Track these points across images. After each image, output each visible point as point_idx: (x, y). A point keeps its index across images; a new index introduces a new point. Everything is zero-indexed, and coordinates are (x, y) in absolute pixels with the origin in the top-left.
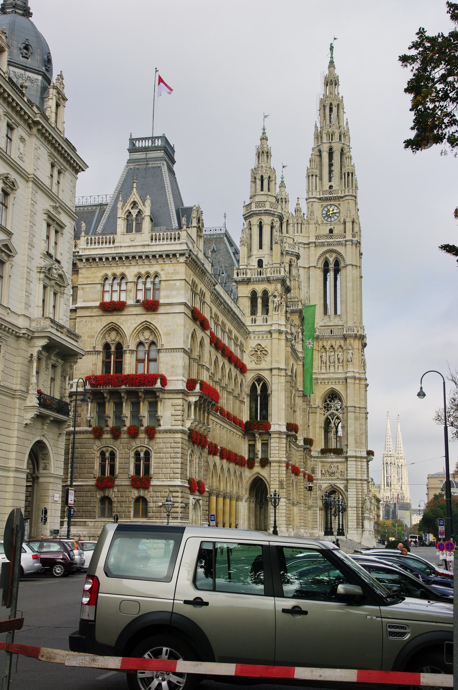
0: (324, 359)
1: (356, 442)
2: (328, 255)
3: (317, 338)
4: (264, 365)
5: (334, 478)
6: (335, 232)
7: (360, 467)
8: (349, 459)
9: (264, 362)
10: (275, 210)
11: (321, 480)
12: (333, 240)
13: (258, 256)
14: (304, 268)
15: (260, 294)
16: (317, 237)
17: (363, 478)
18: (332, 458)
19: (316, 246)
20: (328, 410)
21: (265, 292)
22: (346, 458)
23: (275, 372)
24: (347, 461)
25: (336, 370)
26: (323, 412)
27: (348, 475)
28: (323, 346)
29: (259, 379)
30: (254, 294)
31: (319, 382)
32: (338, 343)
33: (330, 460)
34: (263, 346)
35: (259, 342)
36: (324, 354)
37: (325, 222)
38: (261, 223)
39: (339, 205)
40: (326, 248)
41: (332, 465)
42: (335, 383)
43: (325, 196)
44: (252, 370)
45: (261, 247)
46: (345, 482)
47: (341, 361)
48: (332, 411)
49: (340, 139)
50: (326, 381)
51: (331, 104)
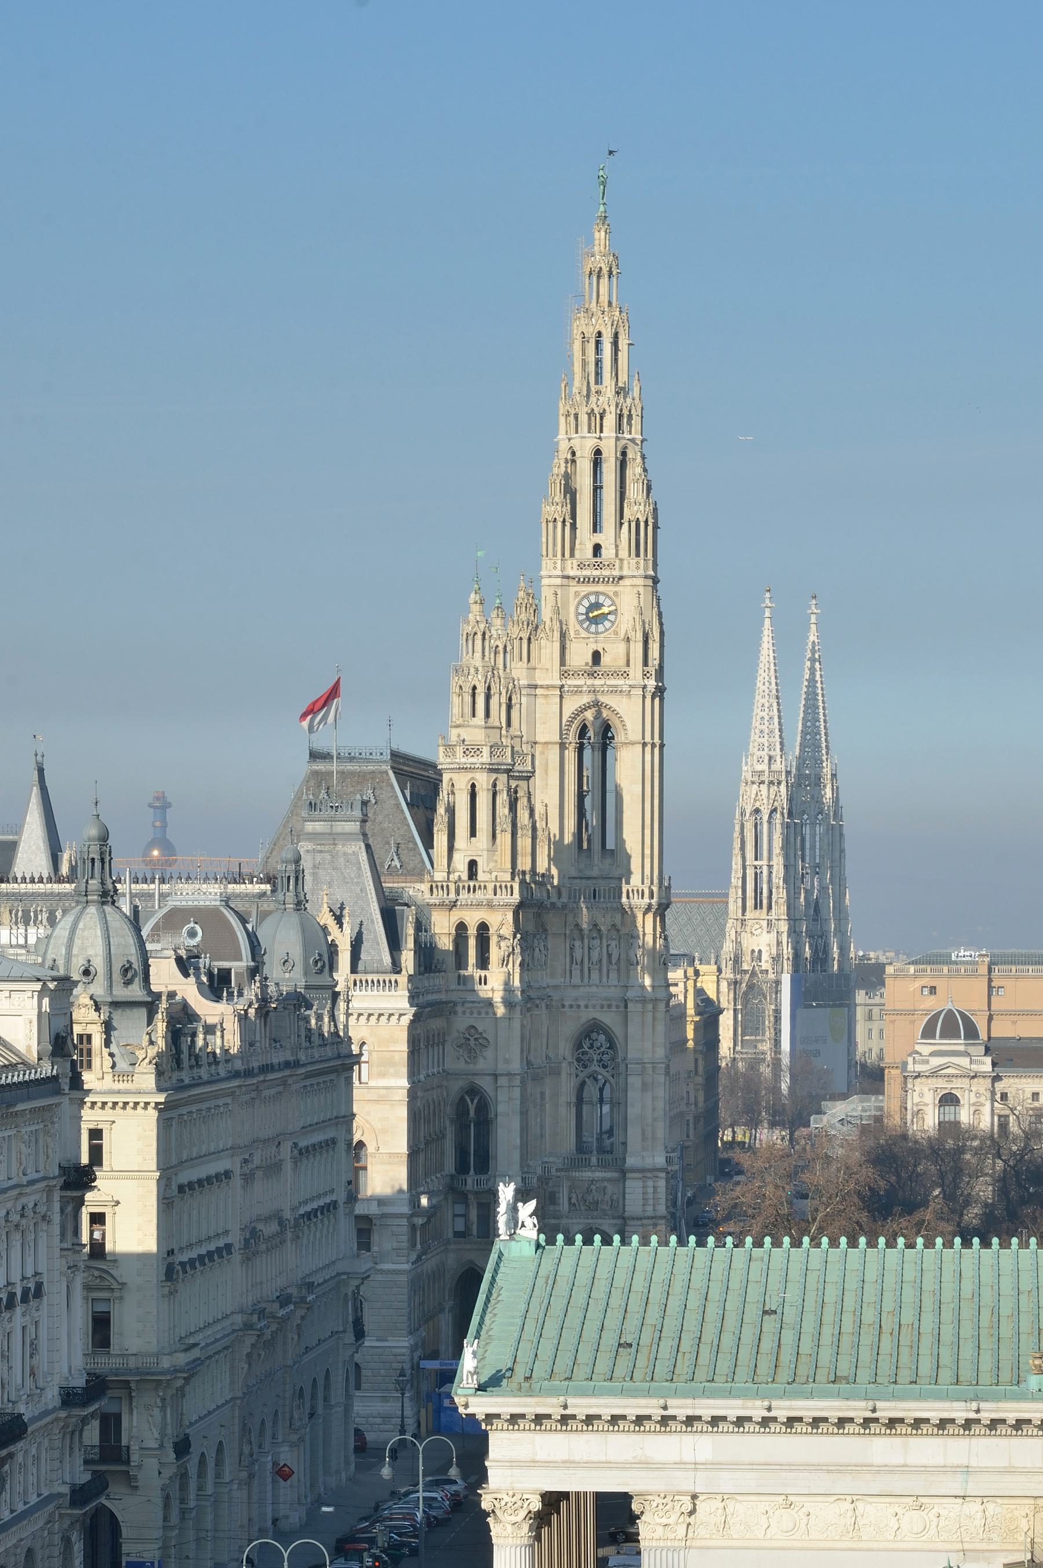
0: (578, 954)
1: (644, 1138)
4: (482, 1065)
5: (596, 1213)
6: (605, 659)
7: (650, 1190)
8: (628, 1175)
9: (481, 1060)
10: (499, 760)
12: (602, 682)
13: (469, 853)
15: (472, 931)
16: (564, 674)
17: (658, 1214)
20: (585, 1066)
21: (483, 927)
22: (624, 1173)
23: (502, 1081)
26: (573, 1071)
29: (473, 1091)
30: (461, 927)
34: (480, 1030)
35: (472, 1022)
36: (578, 943)
37: (584, 634)
38: (473, 786)
45: (473, 833)
46: (619, 1222)
47: (614, 960)
49: (619, 428)
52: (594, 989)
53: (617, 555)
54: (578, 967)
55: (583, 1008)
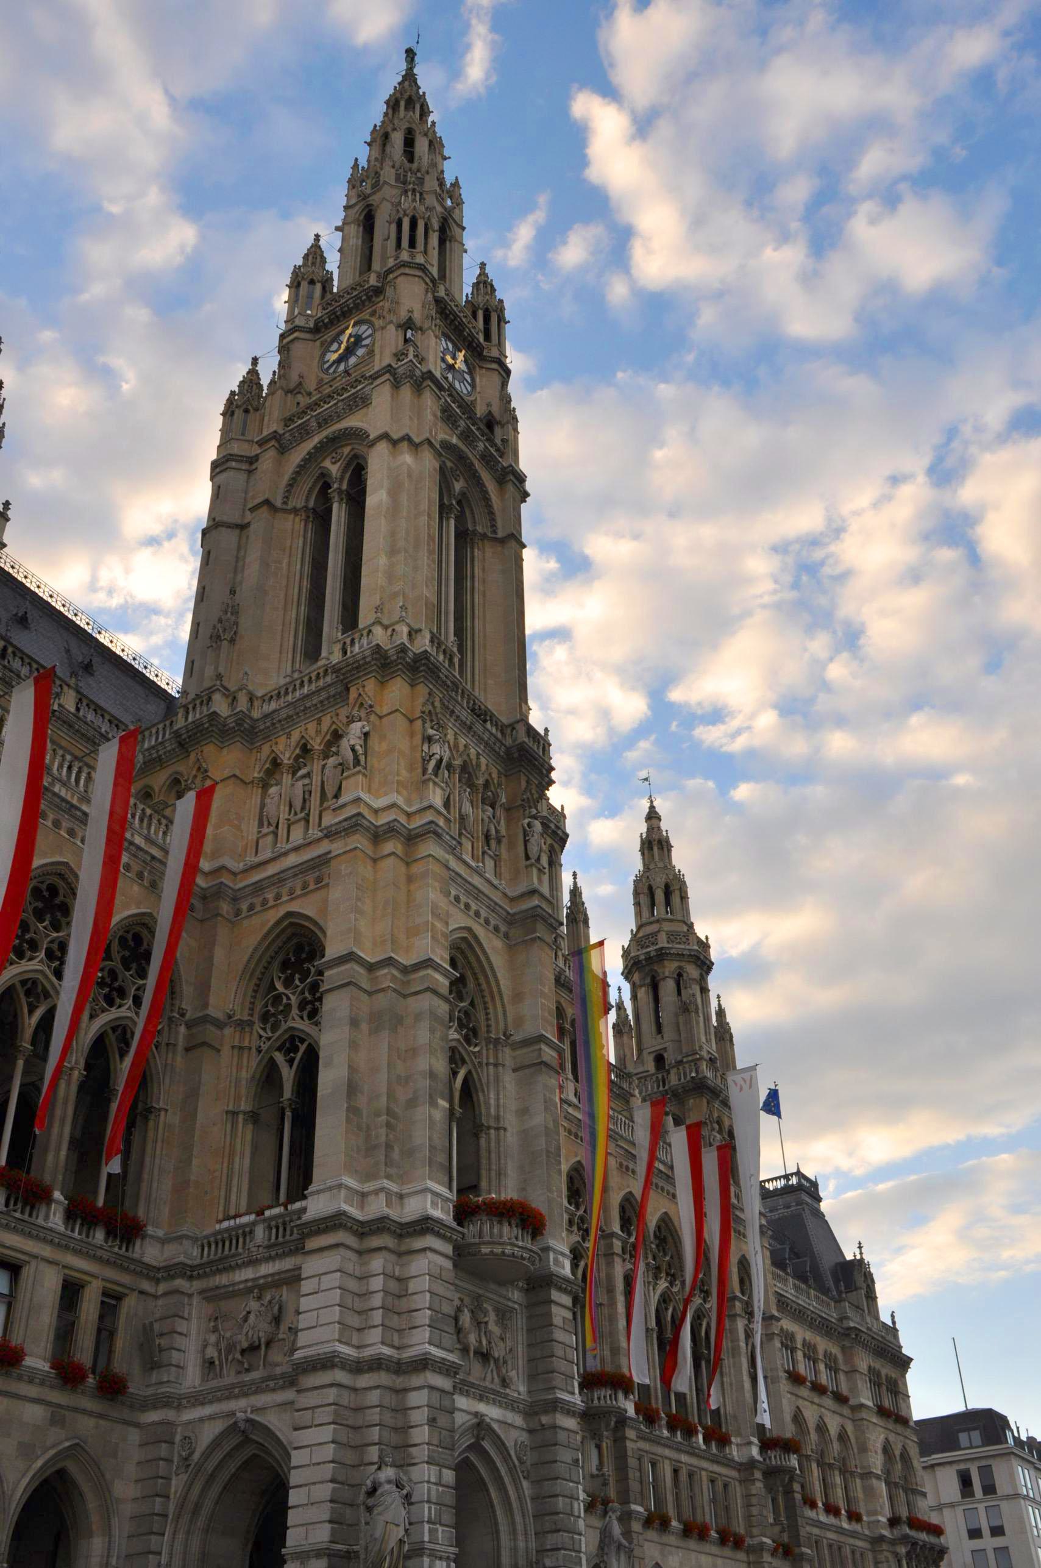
0: (270, 808)
3: (248, 732)
11: (197, 1399)
14: (243, 527)
32: (325, 726)
40: (316, 440)
50: (270, 896)
55: (271, 903)
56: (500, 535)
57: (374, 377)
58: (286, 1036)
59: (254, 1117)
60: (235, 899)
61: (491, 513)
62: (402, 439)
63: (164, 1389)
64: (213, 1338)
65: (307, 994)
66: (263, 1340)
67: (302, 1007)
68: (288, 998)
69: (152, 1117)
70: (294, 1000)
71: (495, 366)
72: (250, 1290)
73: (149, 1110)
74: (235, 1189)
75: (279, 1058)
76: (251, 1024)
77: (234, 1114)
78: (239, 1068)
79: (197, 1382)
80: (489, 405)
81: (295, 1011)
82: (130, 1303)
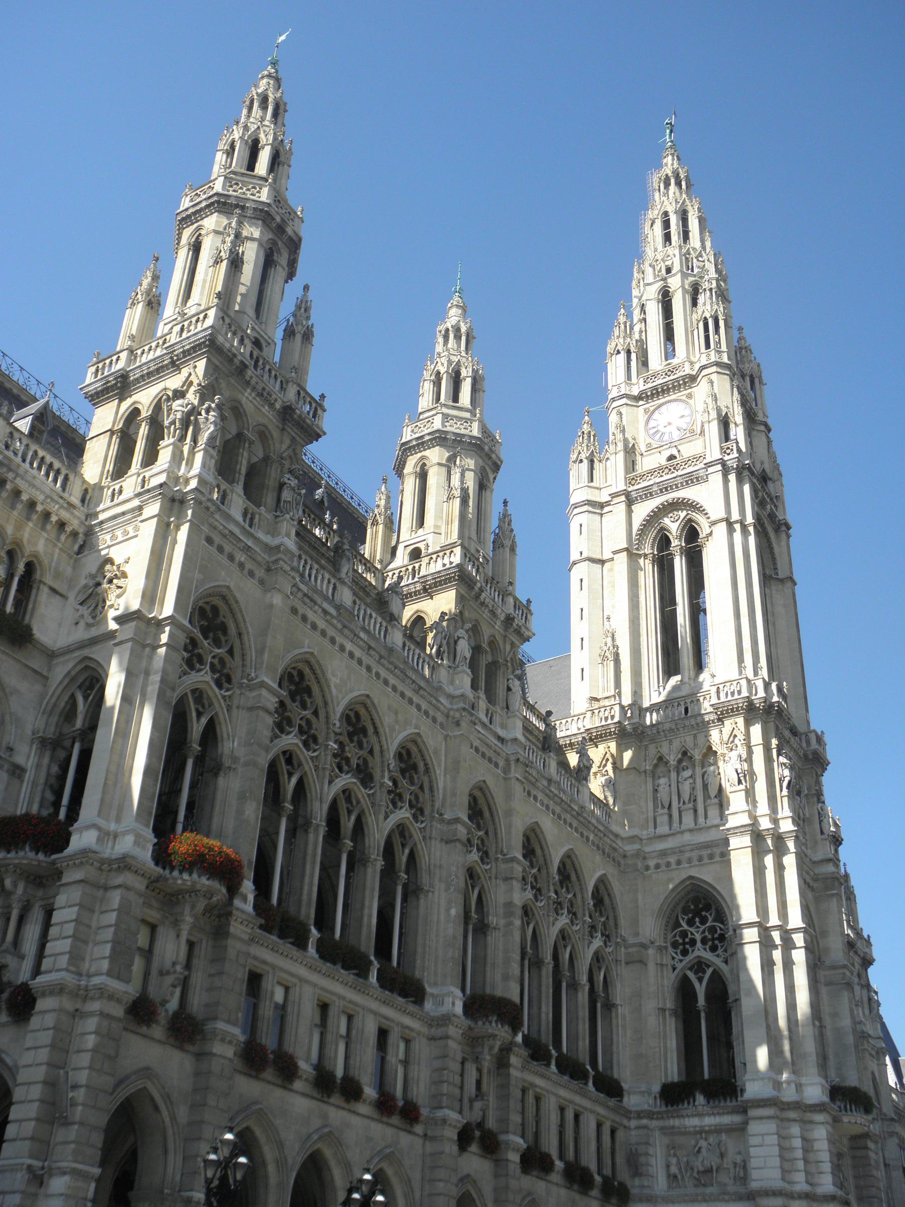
0: (663, 794)
2: (667, 521)
5: (709, 1190)
7: (797, 1143)
14: (602, 562)
16: (630, 481)
18: (701, 1117)
19: (630, 502)
20: (685, 953)
24: (746, 1123)
25: (701, 820)
27: (755, 1174)
28: (660, 759)
31: (652, 863)
33: (695, 1122)
39: (690, 396)
41: (703, 1143)
42: (700, 859)
43: (650, 385)
44: (68, 650)
48: (697, 953)
50: (672, 859)
51: (666, 214)
52: (687, 837)
53: (688, 357)
54: (666, 811)
55: (674, 866)
56: (781, 576)
57: (708, 465)
58: (696, 961)
59: (675, 1013)
60: (645, 858)
61: (774, 559)
62: (736, 522)
63: (646, 1191)
64: (674, 1161)
65: (707, 933)
66: (714, 1168)
67: (704, 941)
68: (692, 934)
69: (614, 1010)
70: (698, 937)
71: (762, 428)
72: (700, 1133)
73: (614, 1005)
74: (669, 1060)
75: (691, 975)
76: (666, 948)
77: (663, 1010)
78: (662, 977)
79: (666, 1188)
80: (762, 463)
81: (699, 944)
82: (620, 1134)
